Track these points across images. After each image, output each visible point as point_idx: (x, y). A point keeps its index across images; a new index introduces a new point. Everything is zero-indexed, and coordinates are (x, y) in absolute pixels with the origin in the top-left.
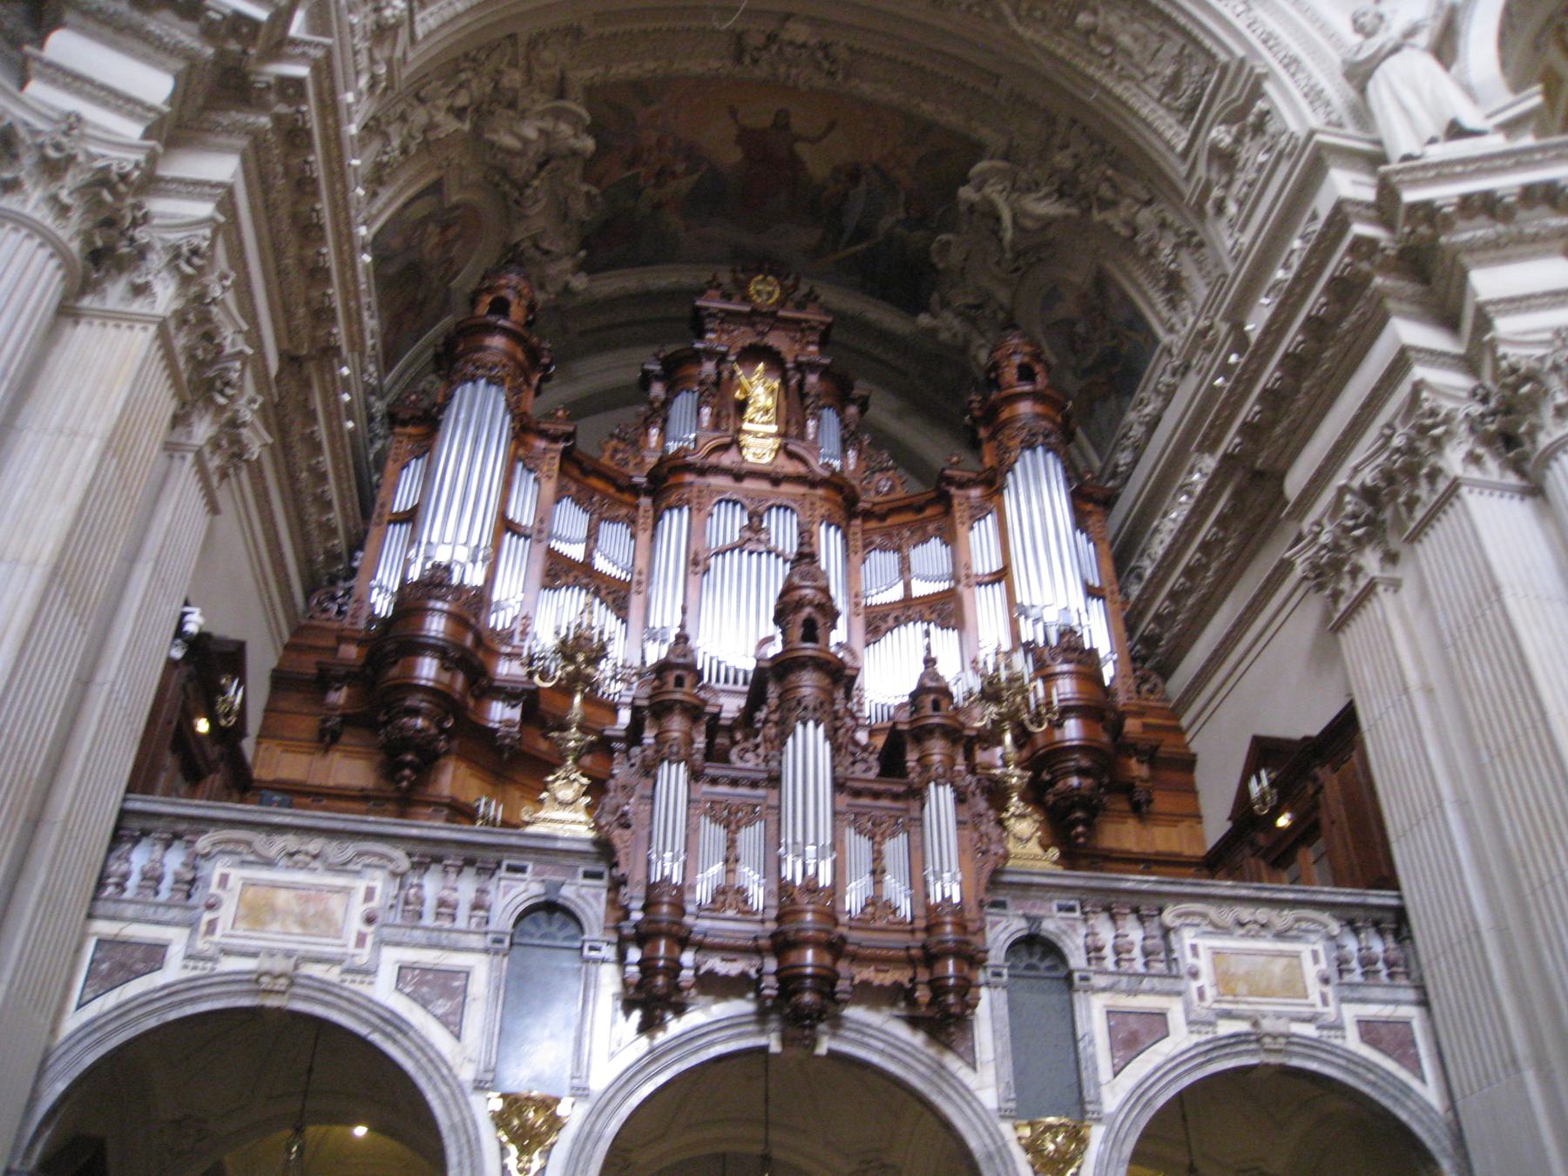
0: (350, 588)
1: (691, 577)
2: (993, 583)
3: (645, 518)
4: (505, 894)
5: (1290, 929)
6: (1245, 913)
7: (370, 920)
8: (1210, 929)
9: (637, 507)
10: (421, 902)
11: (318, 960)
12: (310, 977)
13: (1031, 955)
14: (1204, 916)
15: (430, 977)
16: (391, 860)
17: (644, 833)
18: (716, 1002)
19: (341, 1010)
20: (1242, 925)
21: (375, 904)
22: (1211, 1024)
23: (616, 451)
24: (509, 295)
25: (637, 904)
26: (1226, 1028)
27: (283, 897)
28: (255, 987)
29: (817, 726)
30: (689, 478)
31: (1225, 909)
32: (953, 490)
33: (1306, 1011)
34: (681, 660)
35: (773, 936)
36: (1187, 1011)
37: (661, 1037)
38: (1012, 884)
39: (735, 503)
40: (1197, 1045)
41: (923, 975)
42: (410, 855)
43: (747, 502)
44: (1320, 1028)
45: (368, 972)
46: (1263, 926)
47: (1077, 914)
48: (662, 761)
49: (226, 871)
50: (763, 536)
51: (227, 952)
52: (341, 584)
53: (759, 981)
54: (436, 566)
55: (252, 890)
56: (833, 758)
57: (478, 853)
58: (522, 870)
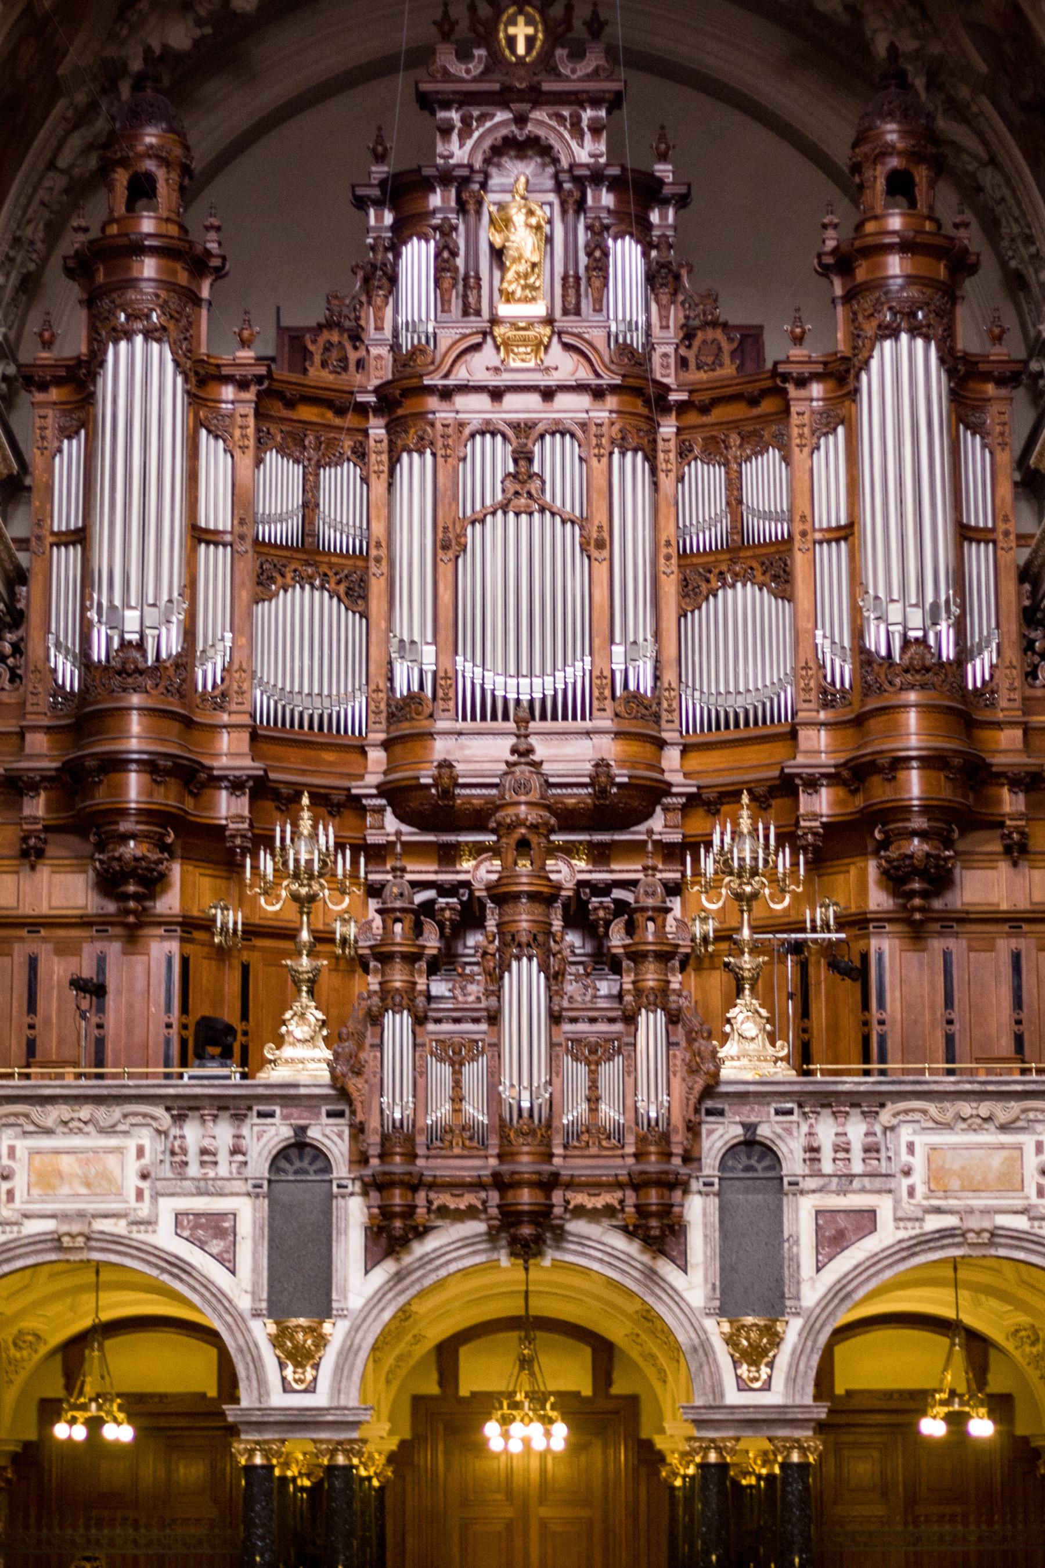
0: (22, 639)
1: (441, 566)
2: (838, 541)
3: (378, 460)
4: (258, 1139)
5: (1018, 1119)
6: (966, 1108)
7: (144, 1176)
8: (931, 1124)
9: (365, 433)
10: (184, 1152)
11: (106, 1216)
12: (102, 1233)
13: (749, 1157)
14: (924, 1112)
15: (203, 1220)
16: (154, 1118)
17: (377, 1080)
18: (452, 1224)
19: (132, 1256)
20: (964, 1120)
21: (146, 1160)
22: (917, 1219)
23: (328, 347)
24: (150, 165)
25: (374, 1151)
26: (934, 1223)
27: (66, 1163)
28: (56, 1244)
29: (530, 959)
30: (433, 402)
31: (947, 1104)
32: (793, 392)
33: (1019, 1204)
34: (398, 904)
35: (495, 1175)
36: (895, 1209)
37: (407, 1260)
38: (727, 1094)
39: (493, 434)
40: (900, 1241)
41: (631, 1197)
42: (168, 1109)
43: (510, 433)
44: (1030, 1219)
45: (149, 1223)
46: (985, 1120)
47: (794, 1118)
48: (386, 1010)
49: (12, 1142)
50: (534, 486)
51: (26, 1216)
52: (8, 636)
53: (485, 1210)
54: (125, 645)
55: (38, 1157)
56: (548, 988)
57: (231, 1103)
58: (271, 1115)
